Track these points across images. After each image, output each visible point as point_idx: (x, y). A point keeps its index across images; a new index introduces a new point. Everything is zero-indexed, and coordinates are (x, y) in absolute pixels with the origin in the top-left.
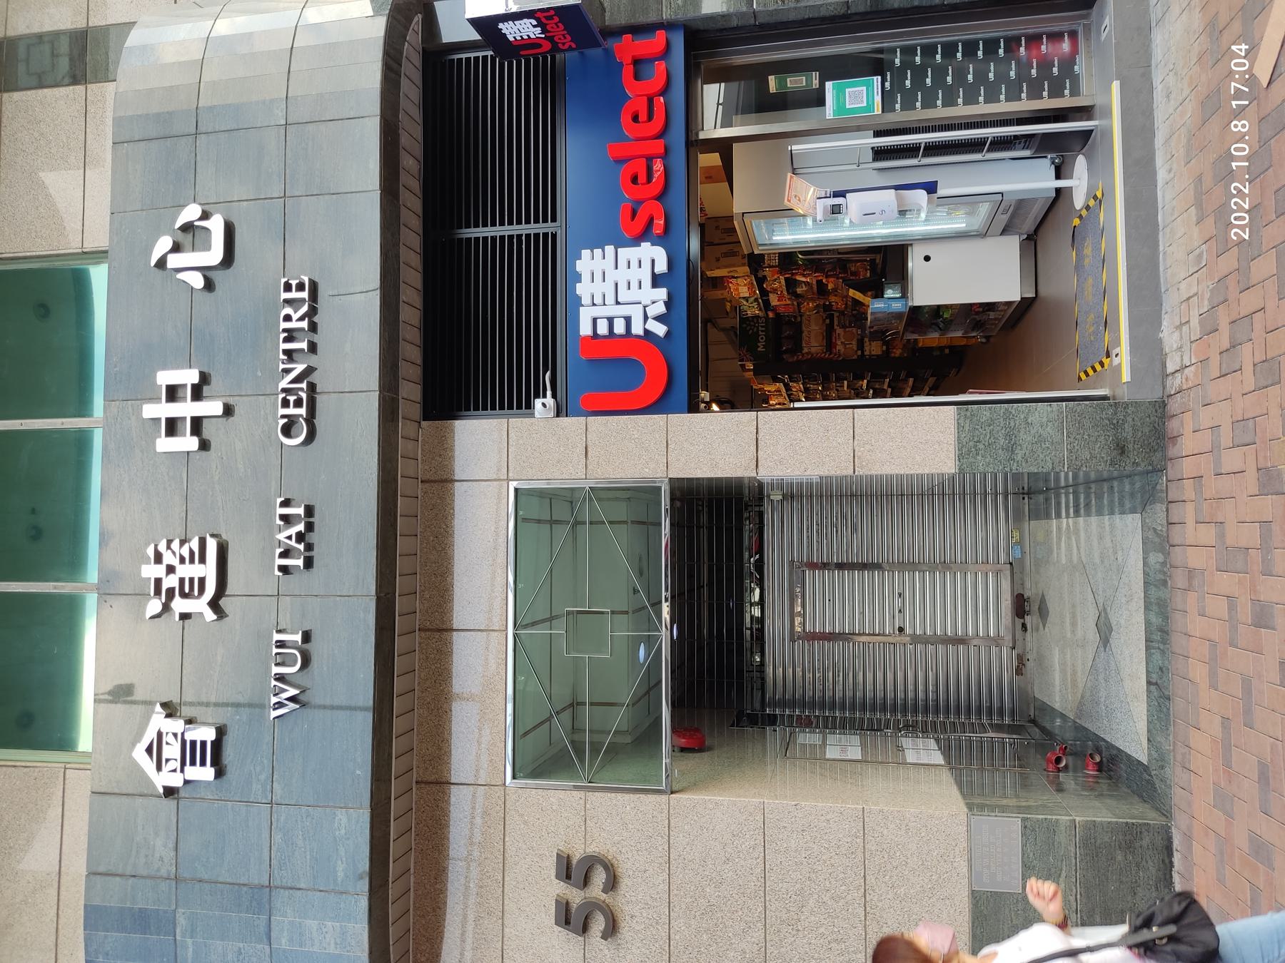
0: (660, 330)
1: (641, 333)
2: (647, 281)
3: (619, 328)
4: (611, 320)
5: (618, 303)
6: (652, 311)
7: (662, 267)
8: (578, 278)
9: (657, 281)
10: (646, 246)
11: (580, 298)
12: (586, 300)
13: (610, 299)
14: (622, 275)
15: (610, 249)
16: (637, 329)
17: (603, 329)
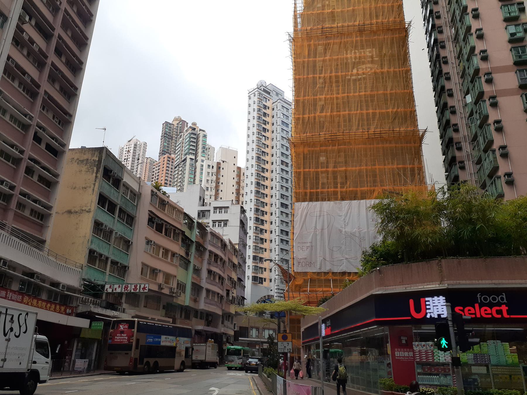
0: (428, 316)
4: (429, 305)
6: (432, 314)
7: (442, 316)
8: (438, 297)
12: (433, 299)
13: (434, 305)
14: (440, 307)
16: (428, 311)
17: (427, 303)
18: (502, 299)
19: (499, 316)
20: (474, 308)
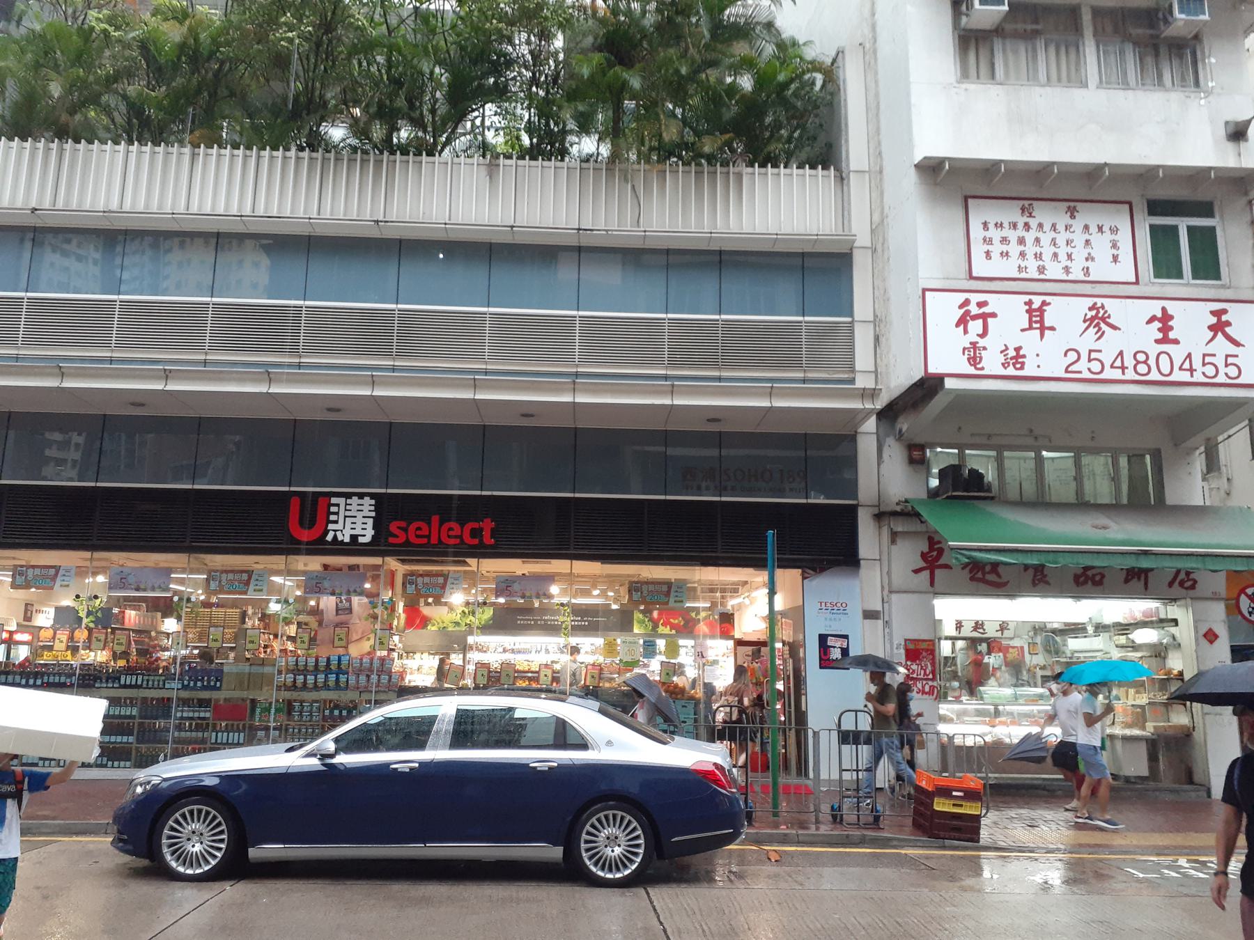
0: (329, 537)
1: (329, 528)
2: (354, 532)
3: (333, 518)
4: (337, 513)
5: (345, 517)
6: (339, 534)
7: (361, 540)
9: (354, 538)
10: (373, 532)
12: (349, 501)
13: (348, 513)
14: (359, 520)
15: (373, 514)
16: (331, 526)
17: (333, 509)
19: (476, 541)
20: (429, 523)
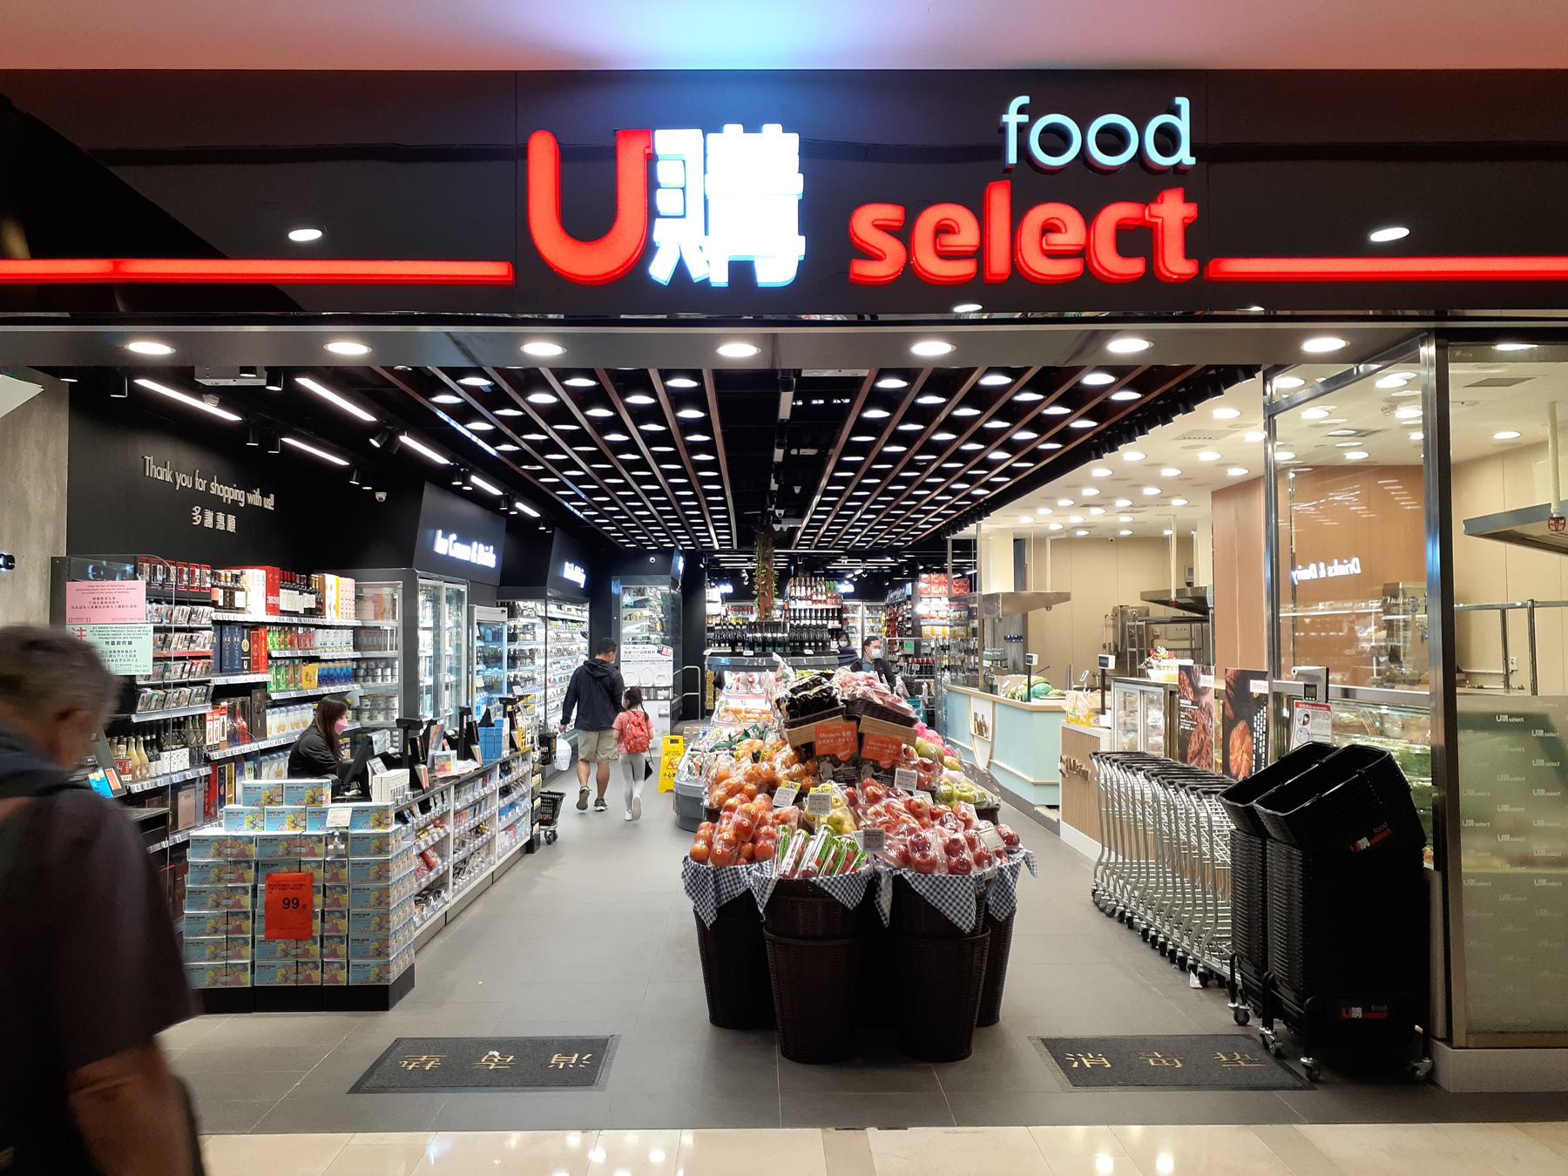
0: (661, 271)
1: (658, 236)
9: (741, 271)
11: (718, 130)
18: (1167, 140)
19: (1134, 267)
